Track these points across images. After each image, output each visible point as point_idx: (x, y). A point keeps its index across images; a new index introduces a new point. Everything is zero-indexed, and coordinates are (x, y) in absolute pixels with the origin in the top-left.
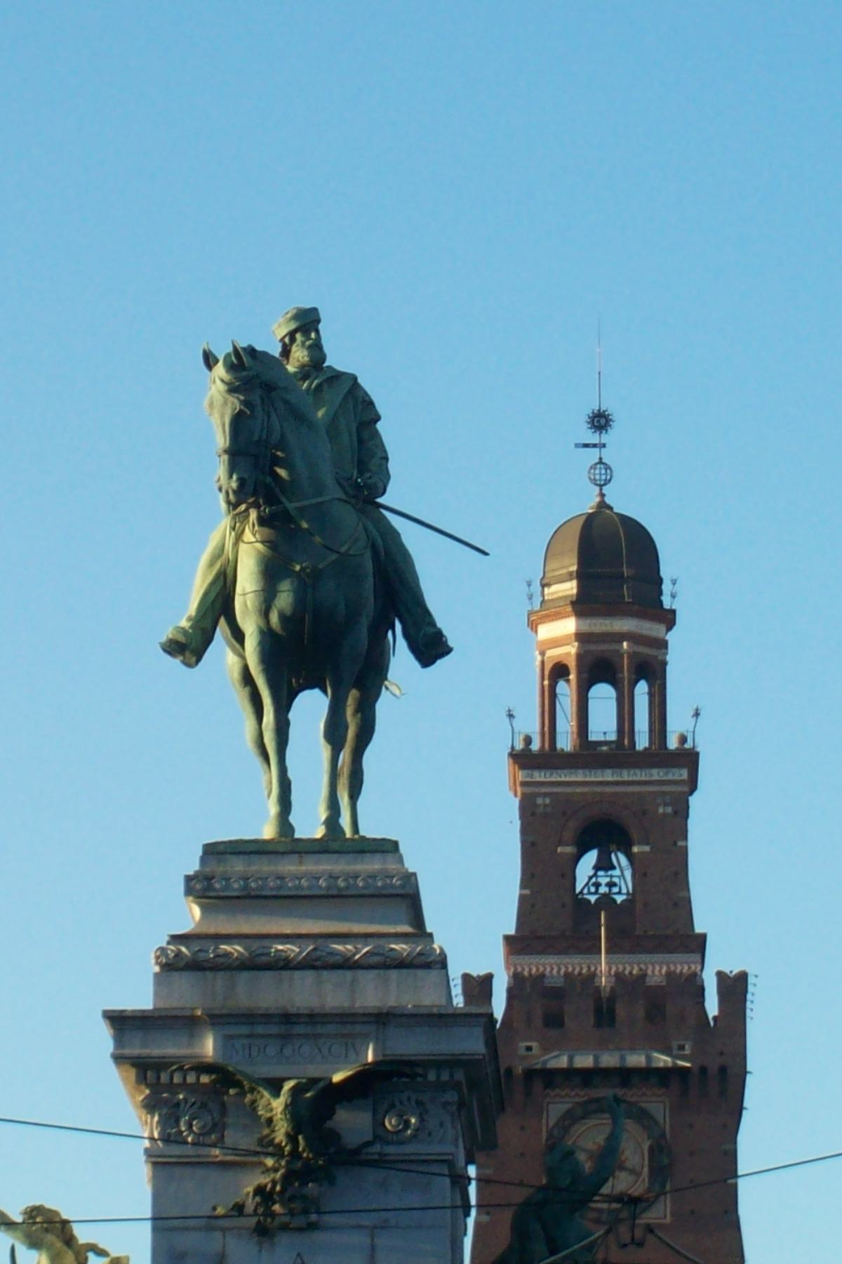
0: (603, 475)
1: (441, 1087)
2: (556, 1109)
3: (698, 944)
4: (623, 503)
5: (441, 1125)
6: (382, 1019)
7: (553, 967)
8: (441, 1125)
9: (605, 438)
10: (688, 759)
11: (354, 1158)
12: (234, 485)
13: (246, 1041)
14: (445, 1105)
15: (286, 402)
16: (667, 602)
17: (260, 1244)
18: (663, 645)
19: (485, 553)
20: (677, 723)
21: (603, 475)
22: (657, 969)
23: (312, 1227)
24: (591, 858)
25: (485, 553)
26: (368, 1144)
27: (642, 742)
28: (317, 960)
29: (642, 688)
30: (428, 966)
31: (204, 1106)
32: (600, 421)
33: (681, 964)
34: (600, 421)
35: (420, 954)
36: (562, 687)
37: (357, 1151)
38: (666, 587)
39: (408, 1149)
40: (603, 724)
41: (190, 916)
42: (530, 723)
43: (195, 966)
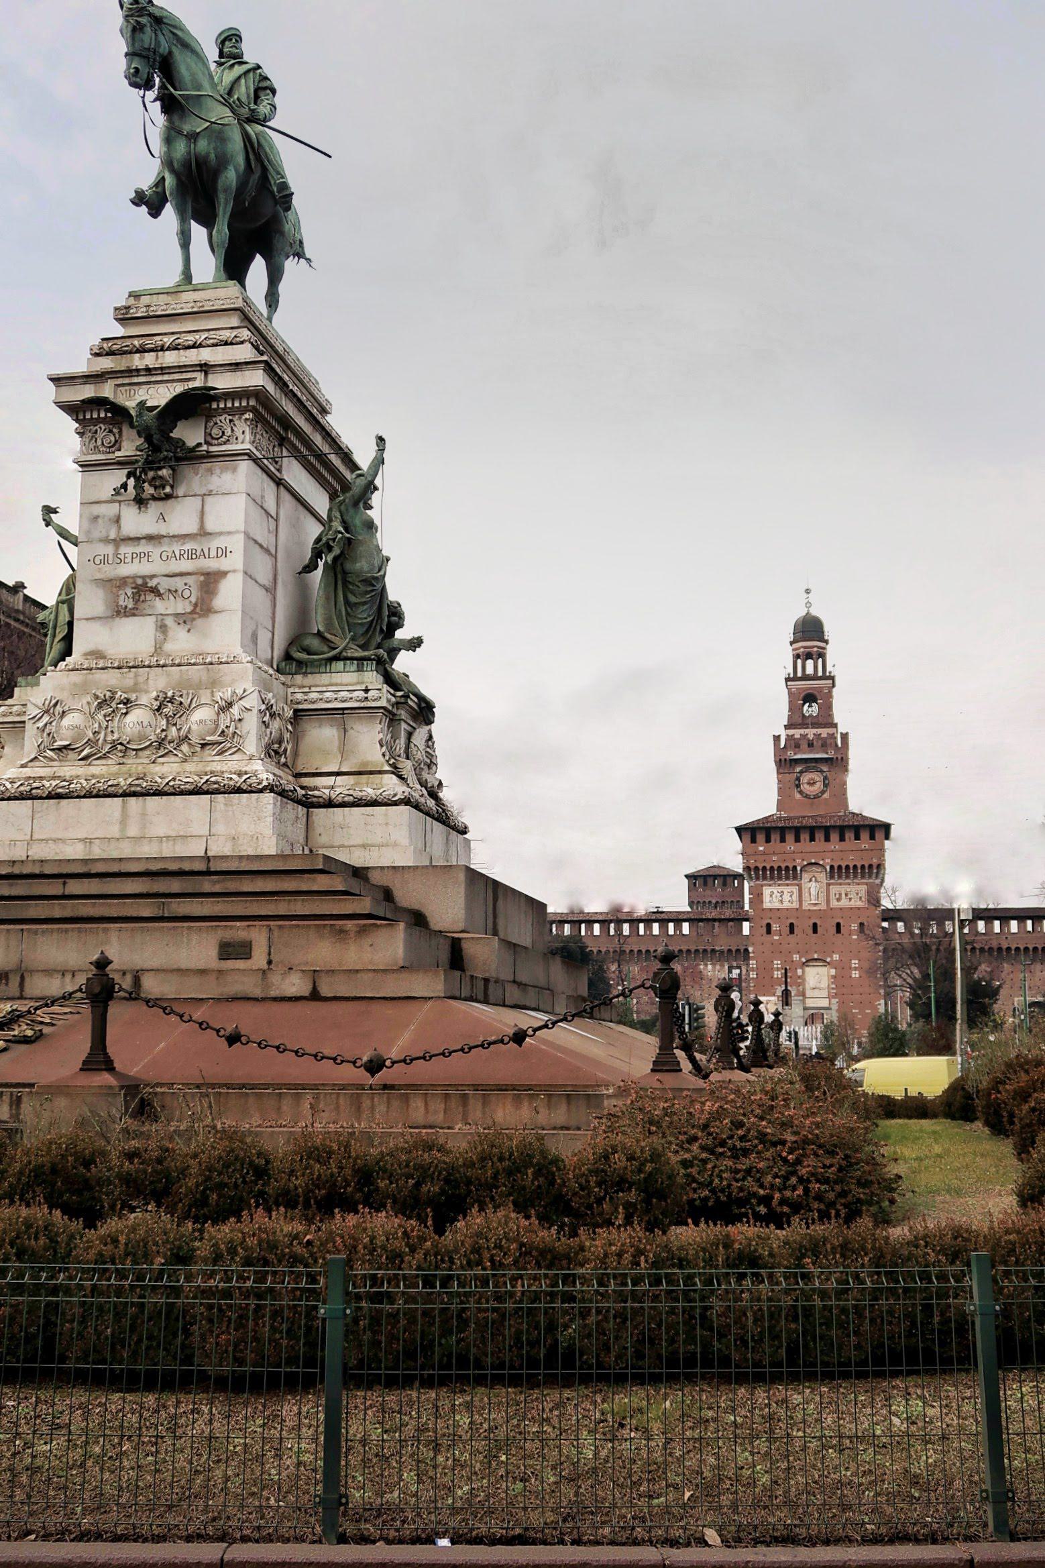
0: (808, 604)
1: (242, 411)
2: (798, 769)
3: (835, 726)
4: (814, 612)
5: (243, 432)
6: (205, 368)
7: (797, 733)
8: (243, 432)
9: (810, 595)
10: (832, 678)
11: (192, 456)
12: (132, 71)
13: (128, 388)
14: (246, 419)
15: (174, 34)
16: (826, 638)
17: (140, 508)
18: (824, 648)
19: (330, 157)
20: (829, 668)
21: (808, 604)
22: (824, 732)
23: (168, 497)
24: (807, 704)
25: (330, 157)
26: (199, 445)
27: (820, 673)
28: (179, 344)
29: (820, 660)
30: (242, 343)
31: (110, 431)
32: (808, 591)
33: (831, 731)
34: (808, 591)
35: (236, 337)
36: (799, 661)
37: (193, 449)
38: (826, 633)
39: (223, 448)
40: (810, 670)
41: (119, 331)
42: (791, 671)
43: (111, 353)
